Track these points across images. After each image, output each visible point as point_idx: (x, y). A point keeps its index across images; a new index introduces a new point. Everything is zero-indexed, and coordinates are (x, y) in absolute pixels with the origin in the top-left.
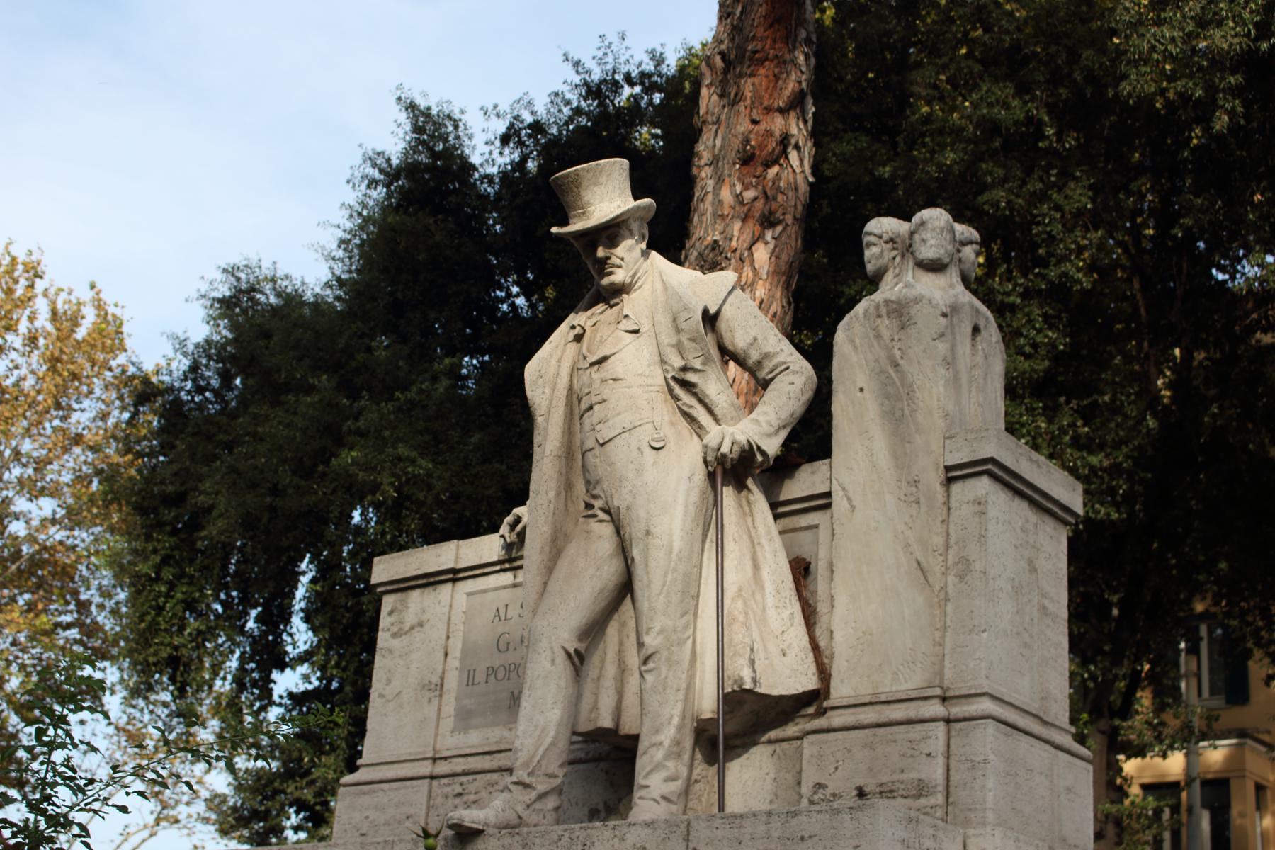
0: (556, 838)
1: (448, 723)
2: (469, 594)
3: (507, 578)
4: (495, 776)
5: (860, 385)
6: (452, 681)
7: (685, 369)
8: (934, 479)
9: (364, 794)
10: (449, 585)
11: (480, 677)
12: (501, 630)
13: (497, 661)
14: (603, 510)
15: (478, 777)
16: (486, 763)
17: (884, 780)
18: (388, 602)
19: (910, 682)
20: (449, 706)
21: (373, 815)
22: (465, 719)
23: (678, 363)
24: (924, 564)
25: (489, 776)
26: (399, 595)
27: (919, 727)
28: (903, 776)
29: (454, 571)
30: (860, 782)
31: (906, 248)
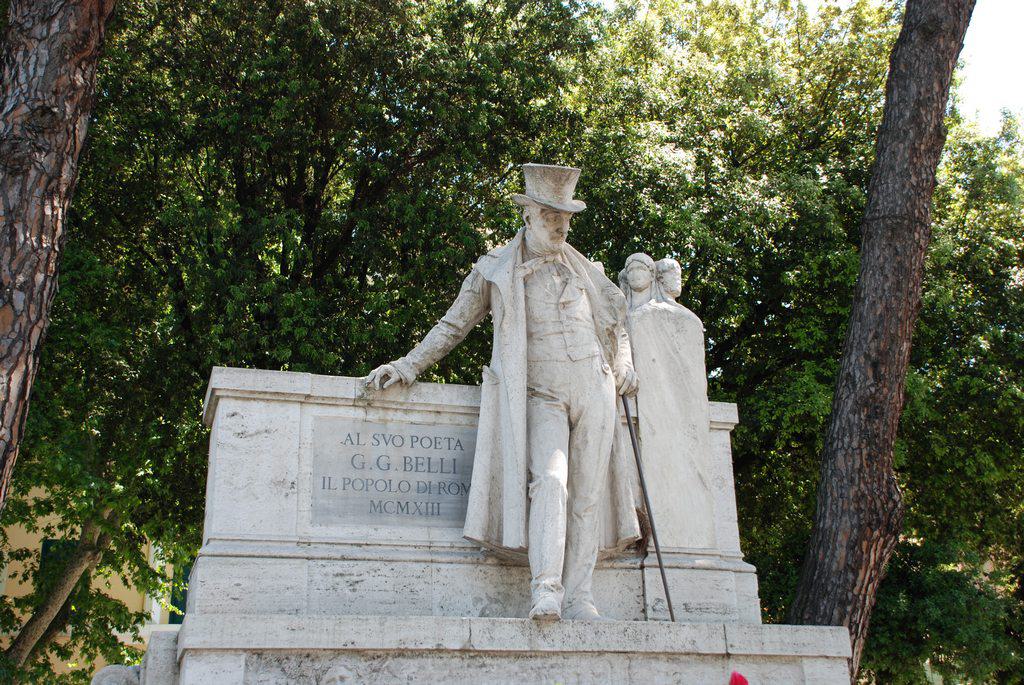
0: (622, 629)
1: (307, 515)
2: (317, 419)
3: (360, 413)
4: (378, 565)
5: (654, 357)
6: (306, 485)
7: (614, 325)
8: (706, 426)
9: (233, 565)
10: (298, 406)
11: (338, 483)
12: (355, 452)
13: (354, 475)
14: (565, 404)
15: (360, 563)
16: (358, 553)
17: (702, 601)
18: (224, 407)
19: (702, 543)
20: (306, 506)
21: (245, 583)
22: (321, 514)
23: (612, 322)
24: (703, 475)
25: (371, 563)
26: (240, 402)
27: (720, 572)
28: (712, 601)
29: (308, 396)
30: (686, 601)
31: (659, 277)
